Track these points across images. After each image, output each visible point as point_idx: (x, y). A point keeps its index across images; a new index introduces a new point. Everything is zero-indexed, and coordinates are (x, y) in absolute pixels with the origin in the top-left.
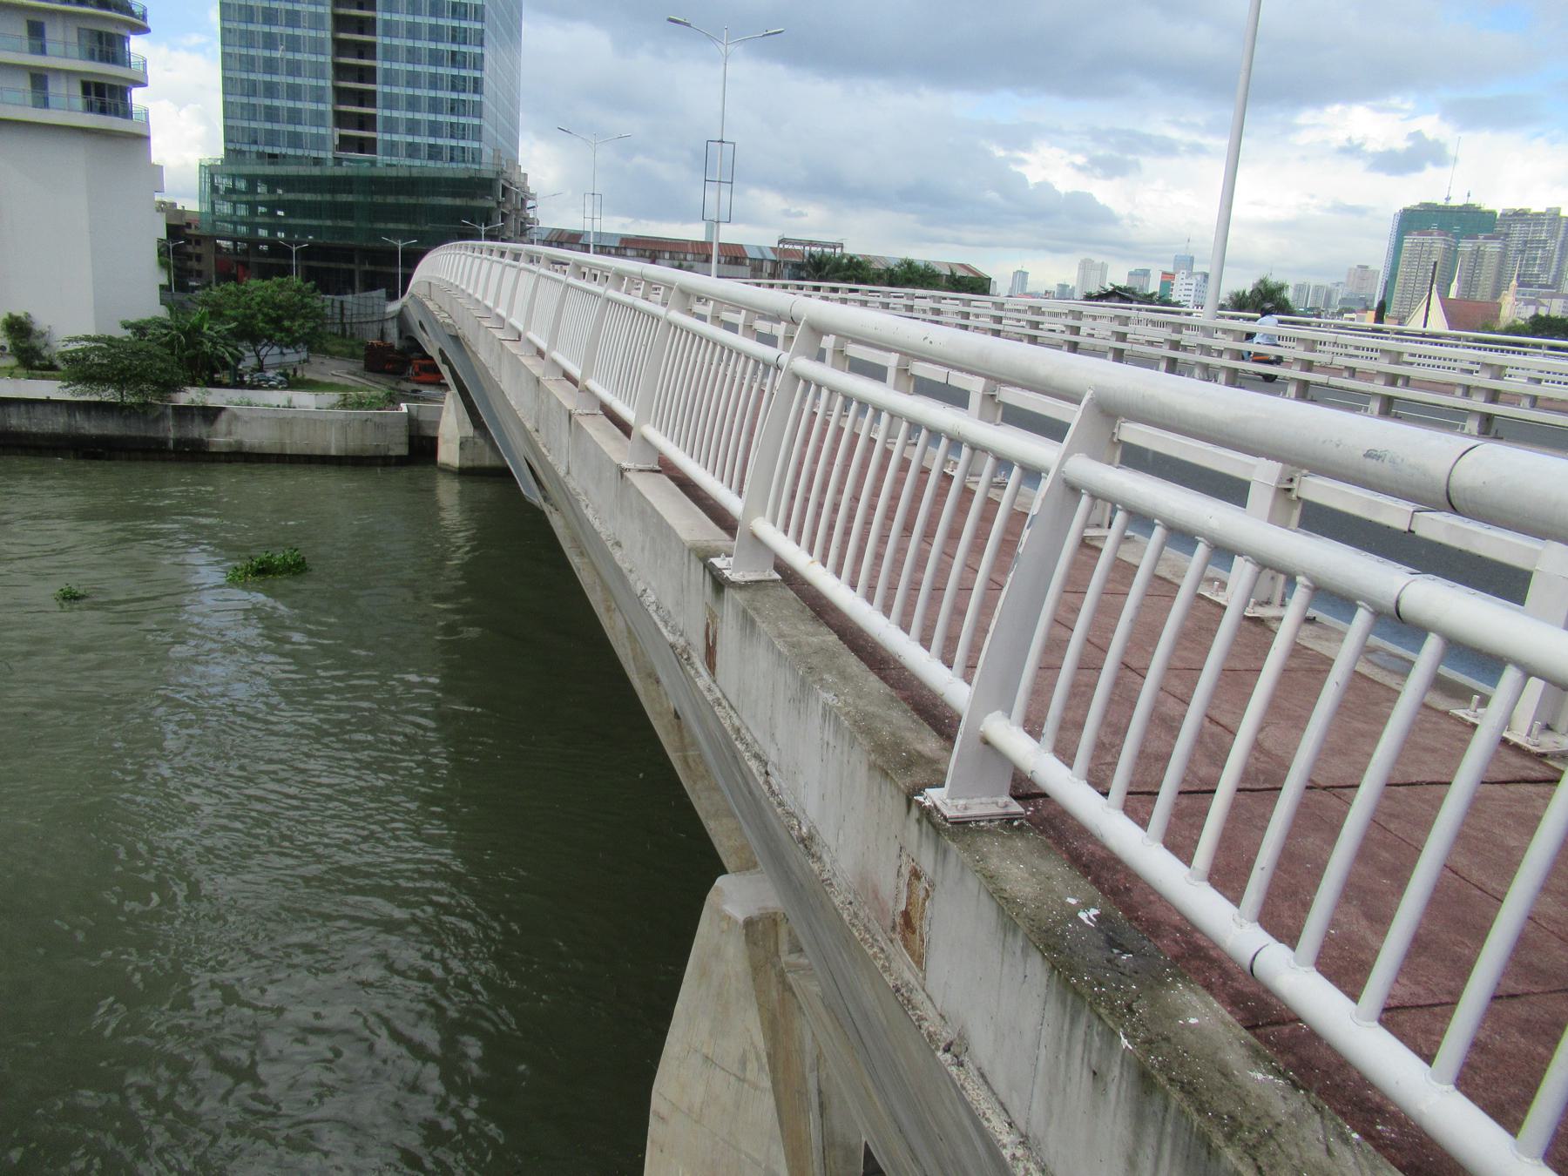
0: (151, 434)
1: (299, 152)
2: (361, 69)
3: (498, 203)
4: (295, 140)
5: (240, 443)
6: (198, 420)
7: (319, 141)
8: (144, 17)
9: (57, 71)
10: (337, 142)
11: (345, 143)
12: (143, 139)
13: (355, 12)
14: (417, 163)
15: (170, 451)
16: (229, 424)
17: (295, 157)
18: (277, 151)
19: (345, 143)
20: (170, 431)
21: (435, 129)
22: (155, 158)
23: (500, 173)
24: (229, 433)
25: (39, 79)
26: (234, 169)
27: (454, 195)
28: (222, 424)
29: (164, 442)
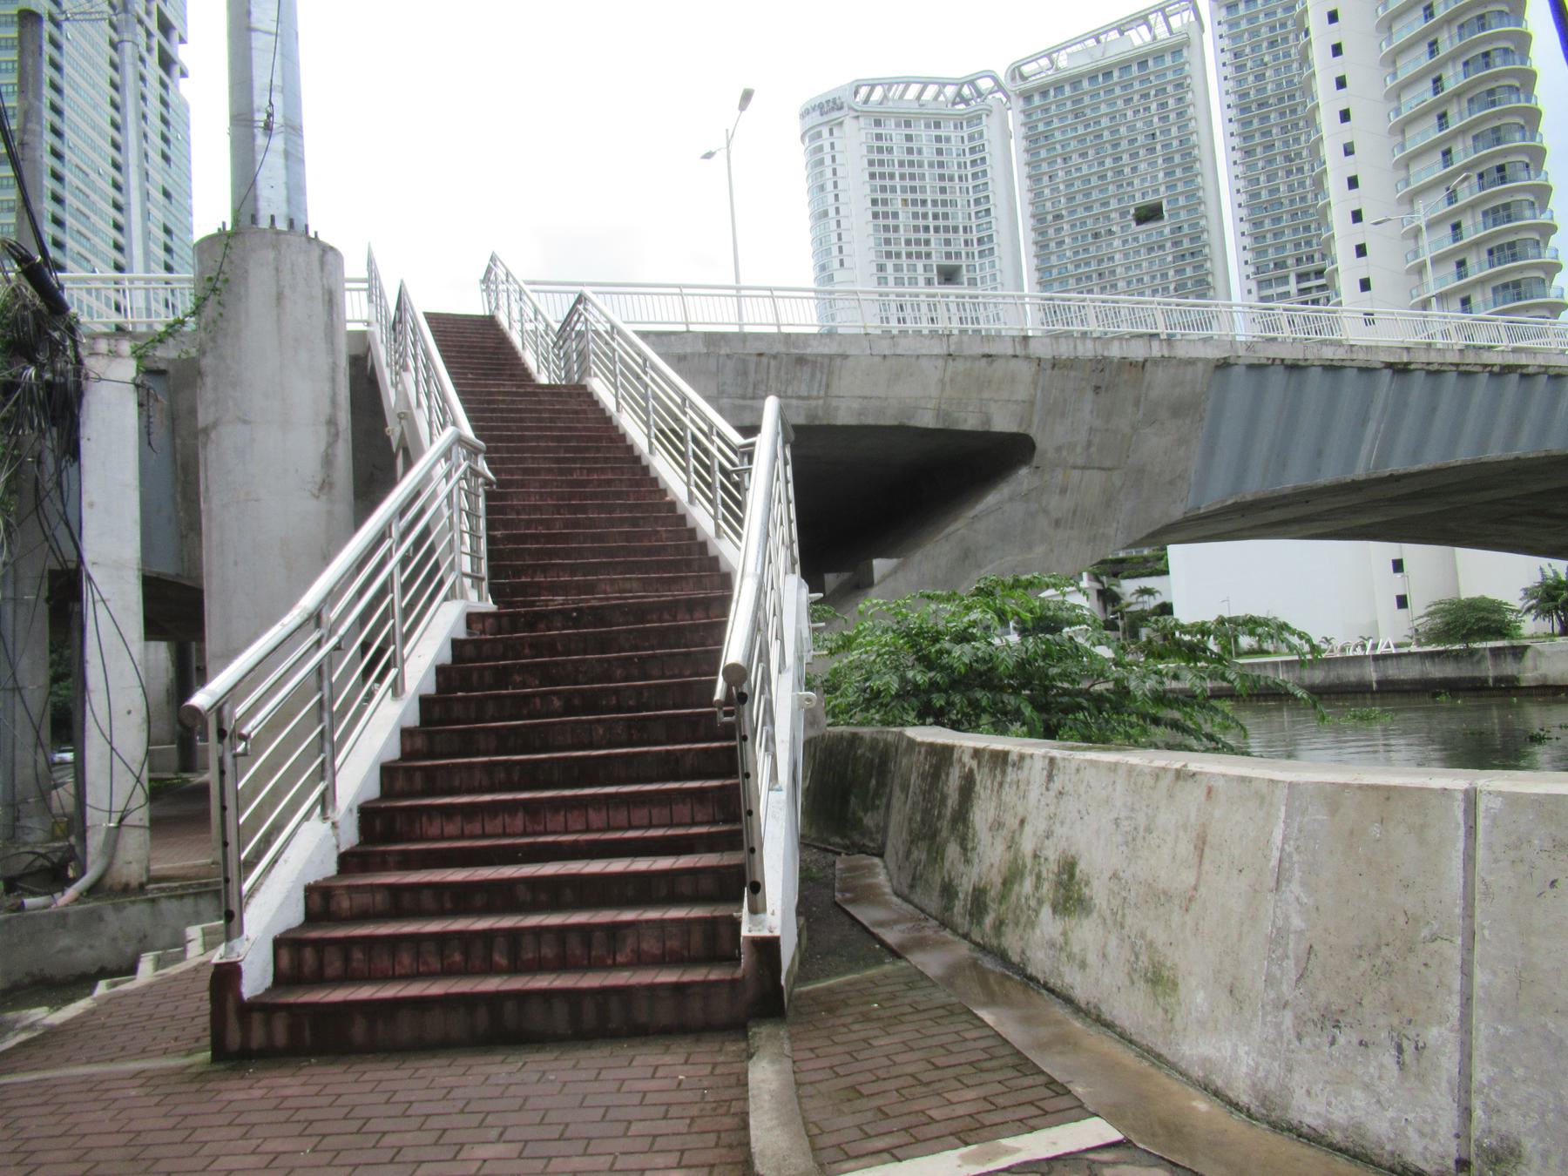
0: (1477, 674)
5: (1545, 677)
6: (1509, 659)
15: (1488, 688)
16: (1535, 659)
20: (1489, 670)
24: (1535, 668)
28: (1528, 660)
29: (1485, 680)
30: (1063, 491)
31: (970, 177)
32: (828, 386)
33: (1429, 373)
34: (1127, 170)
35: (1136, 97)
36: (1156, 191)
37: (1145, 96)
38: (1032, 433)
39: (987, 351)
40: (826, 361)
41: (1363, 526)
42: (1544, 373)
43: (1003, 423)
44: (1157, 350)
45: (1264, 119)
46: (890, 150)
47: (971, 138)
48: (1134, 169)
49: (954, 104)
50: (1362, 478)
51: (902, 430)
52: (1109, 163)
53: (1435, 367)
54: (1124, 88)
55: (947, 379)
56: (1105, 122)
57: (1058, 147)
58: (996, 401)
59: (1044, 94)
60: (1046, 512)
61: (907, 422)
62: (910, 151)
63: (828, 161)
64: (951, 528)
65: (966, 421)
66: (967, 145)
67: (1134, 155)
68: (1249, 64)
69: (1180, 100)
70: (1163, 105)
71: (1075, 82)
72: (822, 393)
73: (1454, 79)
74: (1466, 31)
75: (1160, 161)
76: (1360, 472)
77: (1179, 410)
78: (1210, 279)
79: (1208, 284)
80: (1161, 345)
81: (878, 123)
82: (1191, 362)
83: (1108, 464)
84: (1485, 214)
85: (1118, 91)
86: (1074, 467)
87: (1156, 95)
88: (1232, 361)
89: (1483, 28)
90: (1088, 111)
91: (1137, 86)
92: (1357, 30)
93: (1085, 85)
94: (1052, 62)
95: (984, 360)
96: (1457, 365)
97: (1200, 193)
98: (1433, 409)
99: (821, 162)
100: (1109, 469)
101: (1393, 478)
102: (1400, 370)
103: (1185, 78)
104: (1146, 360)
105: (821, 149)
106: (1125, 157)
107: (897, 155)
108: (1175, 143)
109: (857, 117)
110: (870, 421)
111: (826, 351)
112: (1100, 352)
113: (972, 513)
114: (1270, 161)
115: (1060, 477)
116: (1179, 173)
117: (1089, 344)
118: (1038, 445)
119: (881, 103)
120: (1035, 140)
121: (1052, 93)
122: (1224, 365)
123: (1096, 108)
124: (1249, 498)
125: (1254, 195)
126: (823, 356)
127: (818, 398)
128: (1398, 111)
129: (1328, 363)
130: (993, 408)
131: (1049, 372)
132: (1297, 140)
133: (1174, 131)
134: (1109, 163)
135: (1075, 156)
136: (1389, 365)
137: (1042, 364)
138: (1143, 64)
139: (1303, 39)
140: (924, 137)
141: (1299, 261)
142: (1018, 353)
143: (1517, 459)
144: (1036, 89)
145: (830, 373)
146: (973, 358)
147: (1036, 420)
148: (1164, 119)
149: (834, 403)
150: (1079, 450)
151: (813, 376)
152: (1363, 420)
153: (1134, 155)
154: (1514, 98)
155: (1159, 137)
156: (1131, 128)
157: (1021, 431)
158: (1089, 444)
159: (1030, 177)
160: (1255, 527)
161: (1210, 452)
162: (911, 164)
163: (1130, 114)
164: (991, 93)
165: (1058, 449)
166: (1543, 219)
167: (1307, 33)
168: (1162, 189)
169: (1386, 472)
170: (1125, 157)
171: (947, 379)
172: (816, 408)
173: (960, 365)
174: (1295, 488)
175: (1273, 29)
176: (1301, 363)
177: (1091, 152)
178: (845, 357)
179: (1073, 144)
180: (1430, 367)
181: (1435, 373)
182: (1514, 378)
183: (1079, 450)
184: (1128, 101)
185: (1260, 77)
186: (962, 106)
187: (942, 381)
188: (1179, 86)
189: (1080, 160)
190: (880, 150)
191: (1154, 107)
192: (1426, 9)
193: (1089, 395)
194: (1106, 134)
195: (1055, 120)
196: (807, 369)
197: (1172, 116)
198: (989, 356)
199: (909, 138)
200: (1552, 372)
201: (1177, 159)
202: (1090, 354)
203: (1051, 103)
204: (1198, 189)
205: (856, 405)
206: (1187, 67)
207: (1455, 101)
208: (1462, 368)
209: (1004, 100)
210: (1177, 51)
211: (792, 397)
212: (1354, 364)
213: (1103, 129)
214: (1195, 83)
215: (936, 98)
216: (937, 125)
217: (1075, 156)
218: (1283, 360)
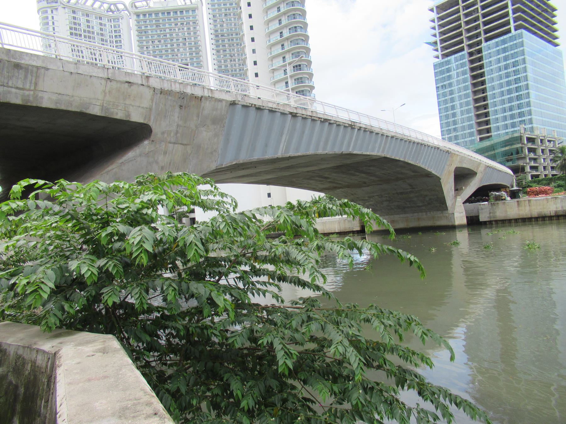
3: (524, 144)
10: (479, 140)
11: (481, 139)
30: (165, 153)
31: (114, 42)
32: (36, 84)
33: (303, 118)
34: (176, 50)
35: (179, 24)
36: (186, 60)
37: (182, 24)
38: (151, 124)
39: (128, 80)
40: (35, 69)
41: (268, 179)
42: (336, 123)
43: (136, 117)
44: (206, 94)
45: (223, 41)
46: (80, 25)
47: (115, 27)
48: (178, 50)
49: (107, 12)
50: (281, 157)
51: (82, 115)
52: (169, 46)
53: (305, 116)
54: (175, 19)
55: (107, 91)
56: (168, 31)
57: (150, 36)
58: (133, 106)
59: (145, 15)
60: (157, 162)
61: (84, 111)
62: (88, 27)
63: (51, 24)
64: (110, 168)
65: (117, 114)
66: (113, 29)
67: (178, 45)
68: (218, 20)
69: (195, 28)
70: (189, 29)
71: (157, 13)
72: (32, 88)
73: (286, 34)
74: (290, 18)
75: (188, 49)
76: (279, 155)
77: (216, 121)
80: (208, 91)
81: (74, 12)
82: (220, 101)
83: (185, 142)
84: (295, 80)
85: (172, 20)
86: (170, 143)
87: (186, 25)
88: (237, 102)
89: (295, 18)
90: (161, 25)
91: (179, 20)
92: (256, 10)
93: (160, 15)
94: (147, 4)
95: (127, 84)
96: (311, 116)
97: (202, 63)
98: (303, 132)
99: (48, 24)
100: (186, 145)
101: (290, 158)
102: (294, 115)
103: (197, 20)
104: (202, 97)
105: (47, 18)
106: (175, 45)
107: (83, 27)
108: (193, 43)
109: (64, 8)
110: (63, 107)
111: (34, 64)
112: (182, 90)
113: (120, 161)
114: (225, 56)
115: (164, 146)
116: (194, 55)
117: (177, 85)
118: (153, 130)
119: (75, 4)
120: (141, 32)
121: (147, 15)
122: (233, 104)
123: (164, 25)
124: (241, 162)
125: (220, 67)
126: (33, 66)
127: (29, 90)
128: (269, 41)
129: (271, 109)
130: (131, 109)
131: (159, 95)
132: (233, 50)
133: (193, 38)
134: (169, 46)
135: (156, 41)
136: (291, 113)
137: (156, 91)
138: (182, 12)
139: (239, 11)
140: (95, 23)
142: (144, 83)
143: (326, 154)
144: (141, 13)
145: (37, 77)
146: (121, 82)
147: (152, 118)
148: (189, 34)
149: (40, 94)
150: (172, 135)
151: (26, 77)
152: (281, 134)
153: (178, 45)
154: (303, 43)
155: (187, 40)
156: (177, 35)
157: (145, 123)
158: (177, 132)
159: (139, 46)
160: (232, 178)
161: (227, 141)
162: (89, 32)
163: (177, 29)
164: (123, 10)
165: (163, 133)
166: (311, 84)
167: (240, 9)
168: (188, 59)
169: (288, 155)
170: (175, 45)
171: (107, 91)
172: (29, 95)
173: (114, 85)
174: (258, 159)
175: (226, 10)
176: (262, 107)
177: (162, 41)
178: (48, 69)
179: (156, 37)
180: (303, 116)
181: (304, 119)
182: (327, 124)
183: (172, 135)
184: (176, 24)
185: (222, 26)
186: (111, 13)
187: (104, 92)
188: (194, 23)
189: (158, 43)
190: (75, 24)
191: (185, 28)
192: (278, 8)
193: (177, 109)
194: (168, 35)
195: (149, 26)
196: (22, 73)
197: (192, 33)
198: (130, 83)
199: (88, 21)
200: (338, 123)
201: (194, 49)
202: (178, 90)
203: (147, 19)
204: (201, 61)
205: (54, 97)
206: (197, 17)
207: (286, 41)
208: (313, 118)
209: (129, 15)
210: (194, 11)
211: (12, 87)
212: (279, 111)
213: (167, 33)
214: (200, 23)
215: (100, 8)
216: (101, 18)
217: (156, 41)
218: (255, 105)
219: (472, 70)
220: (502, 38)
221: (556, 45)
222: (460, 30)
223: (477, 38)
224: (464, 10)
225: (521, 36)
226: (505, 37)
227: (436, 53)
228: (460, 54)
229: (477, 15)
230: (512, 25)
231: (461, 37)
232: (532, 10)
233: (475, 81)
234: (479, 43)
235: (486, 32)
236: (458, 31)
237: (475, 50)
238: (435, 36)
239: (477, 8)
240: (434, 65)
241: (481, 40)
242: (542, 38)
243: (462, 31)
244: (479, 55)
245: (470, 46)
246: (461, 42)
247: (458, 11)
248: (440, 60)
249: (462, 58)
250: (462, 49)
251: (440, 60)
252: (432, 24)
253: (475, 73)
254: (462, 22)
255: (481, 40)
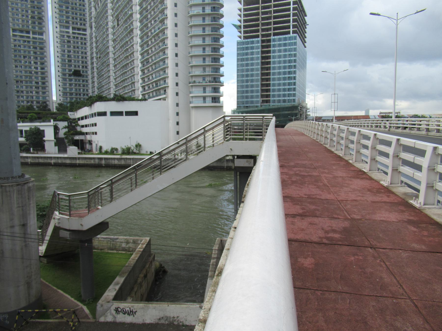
1: (253, 105)
2: (267, 84)
4: (252, 102)
7: (257, 102)
8: (223, 83)
9: (208, 96)
10: (261, 101)
11: (263, 102)
12: (222, 107)
13: (266, 72)
14: (280, 104)
15: (225, 169)
17: (252, 106)
18: (248, 105)
19: (263, 102)
21: (284, 95)
22: (224, 111)
23: (299, 104)
25: (204, 98)
26: (238, 111)
27: (289, 111)
29: (224, 167)
78: (44, 18)
79: (43, 20)
141: (73, 23)
219: (263, 52)
220: (284, 36)
221: (305, 47)
222: (258, 22)
223: (268, 31)
224: (262, 9)
225: (295, 38)
226: (286, 36)
227: (239, 34)
228: (256, 39)
229: (270, 15)
230: (291, 30)
231: (258, 28)
232: (300, 21)
233: (263, 61)
234: (269, 35)
235: (275, 29)
236: (257, 23)
237: (266, 40)
238: (240, 21)
239: (271, 11)
240: (237, 42)
241: (271, 33)
242: (302, 40)
243: (259, 23)
244: (269, 44)
245: (263, 36)
246: (258, 31)
247: (257, 8)
248: (242, 40)
249: (258, 42)
250: (257, 36)
251: (242, 40)
252: (239, 13)
253: (264, 55)
254: (260, 17)
255: (271, 33)
